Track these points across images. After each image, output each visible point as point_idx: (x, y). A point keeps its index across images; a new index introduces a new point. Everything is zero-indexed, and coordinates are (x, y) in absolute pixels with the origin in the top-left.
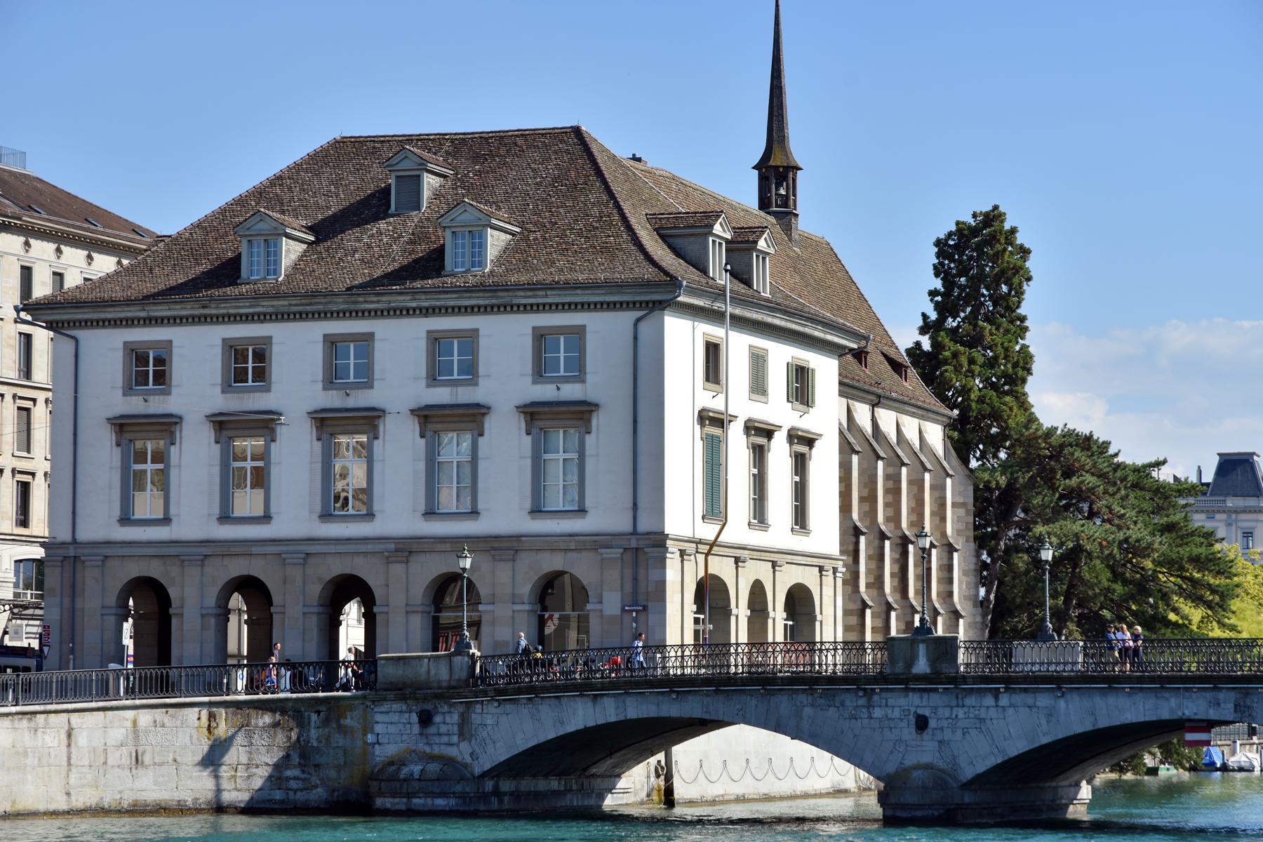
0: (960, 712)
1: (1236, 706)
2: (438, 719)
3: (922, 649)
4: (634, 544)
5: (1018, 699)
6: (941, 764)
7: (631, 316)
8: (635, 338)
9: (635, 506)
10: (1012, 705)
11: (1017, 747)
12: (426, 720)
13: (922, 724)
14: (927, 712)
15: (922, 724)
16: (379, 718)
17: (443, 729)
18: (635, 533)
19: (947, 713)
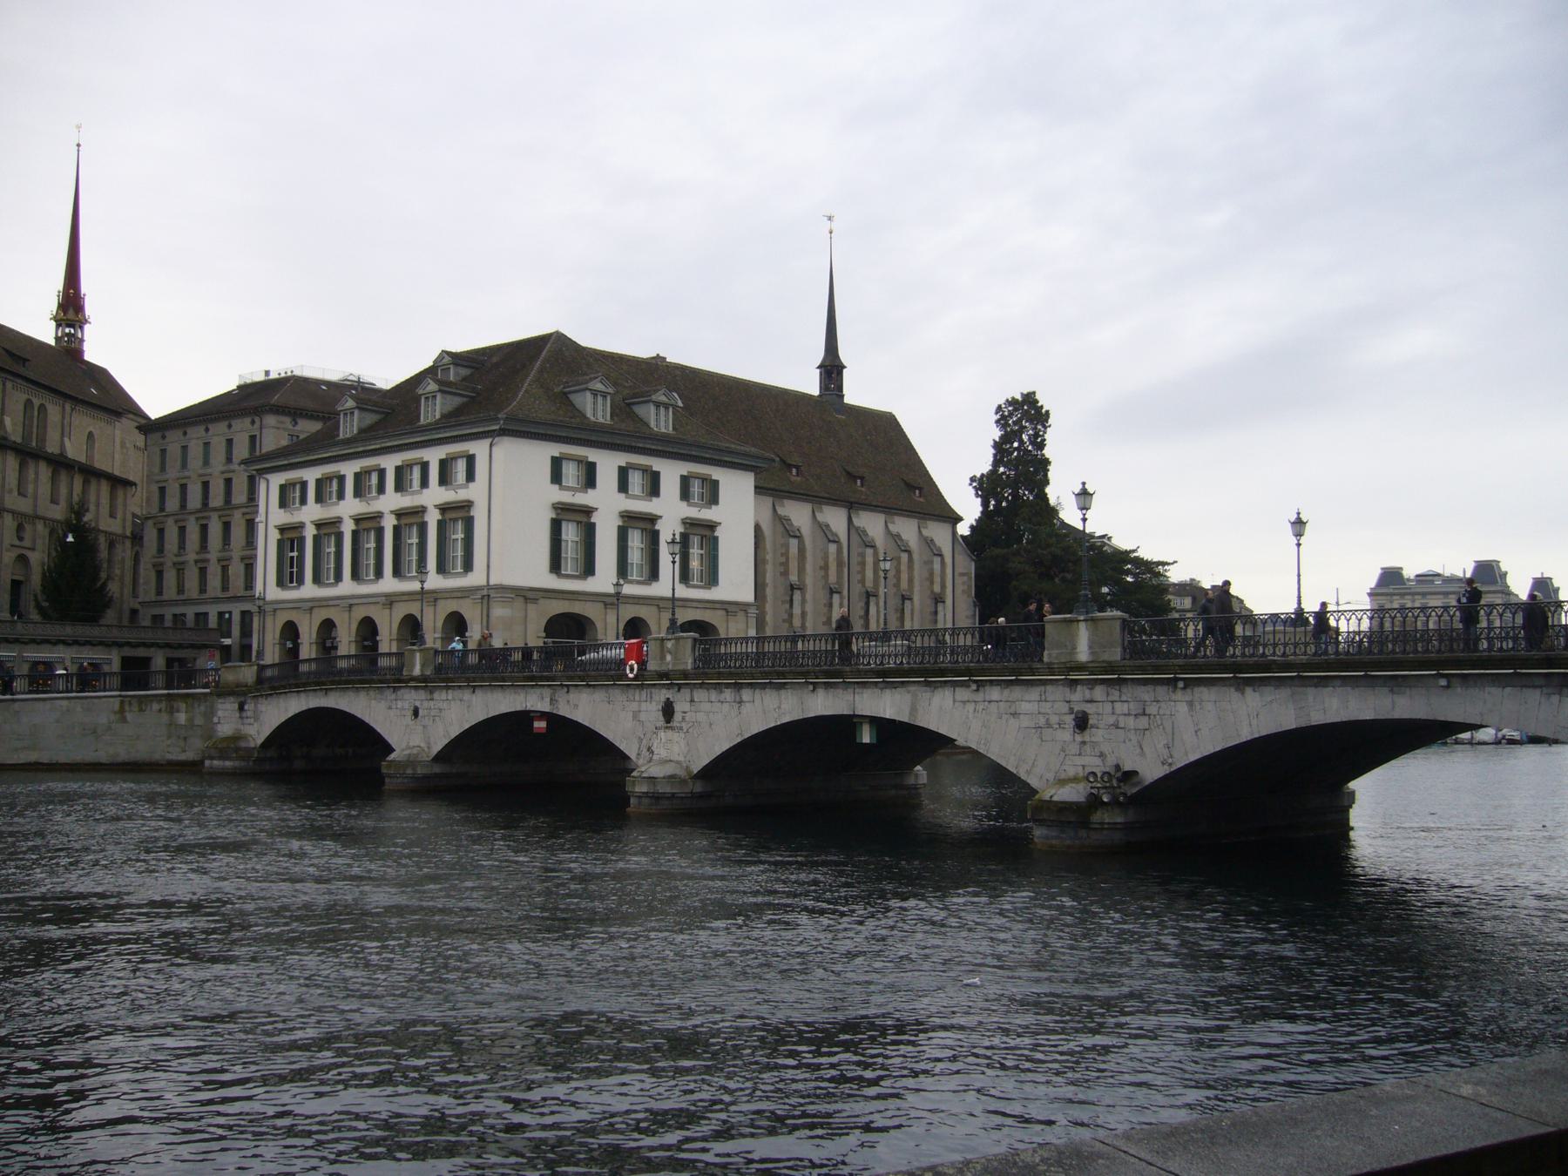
0: (431, 703)
1: (551, 699)
2: (246, 707)
3: (418, 654)
4: (485, 592)
5: (451, 694)
6: (422, 745)
7: (486, 442)
8: (490, 456)
9: (488, 566)
10: (454, 699)
11: (455, 732)
12: (241, 708)
13: (416, 713)
14: (418, 704)
15: (416, 713)
16: (220, 706)
17: (249, 714)
18: (488, 585)
19: (426, 704)
